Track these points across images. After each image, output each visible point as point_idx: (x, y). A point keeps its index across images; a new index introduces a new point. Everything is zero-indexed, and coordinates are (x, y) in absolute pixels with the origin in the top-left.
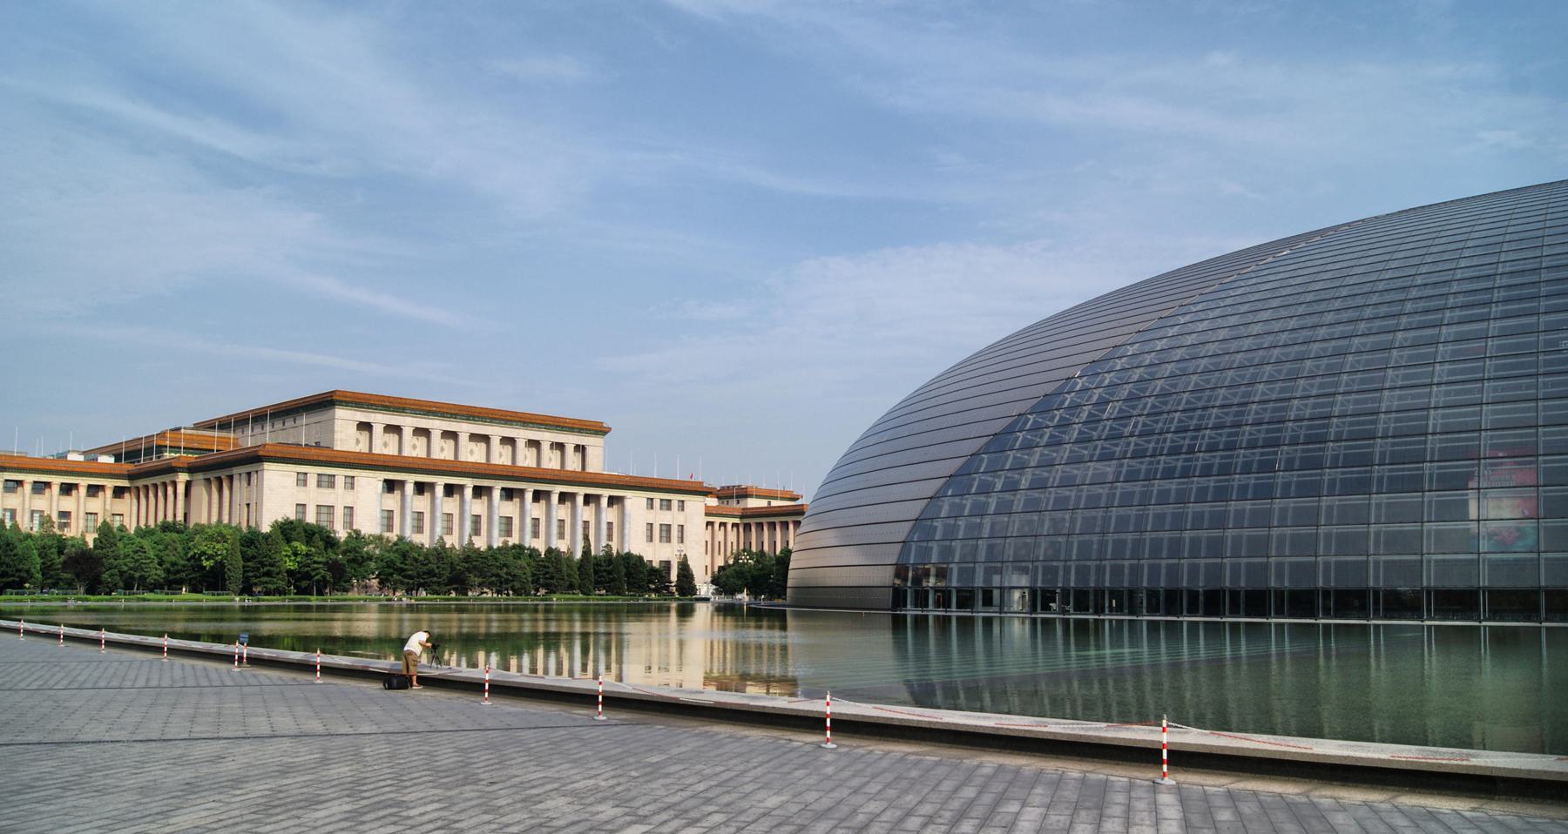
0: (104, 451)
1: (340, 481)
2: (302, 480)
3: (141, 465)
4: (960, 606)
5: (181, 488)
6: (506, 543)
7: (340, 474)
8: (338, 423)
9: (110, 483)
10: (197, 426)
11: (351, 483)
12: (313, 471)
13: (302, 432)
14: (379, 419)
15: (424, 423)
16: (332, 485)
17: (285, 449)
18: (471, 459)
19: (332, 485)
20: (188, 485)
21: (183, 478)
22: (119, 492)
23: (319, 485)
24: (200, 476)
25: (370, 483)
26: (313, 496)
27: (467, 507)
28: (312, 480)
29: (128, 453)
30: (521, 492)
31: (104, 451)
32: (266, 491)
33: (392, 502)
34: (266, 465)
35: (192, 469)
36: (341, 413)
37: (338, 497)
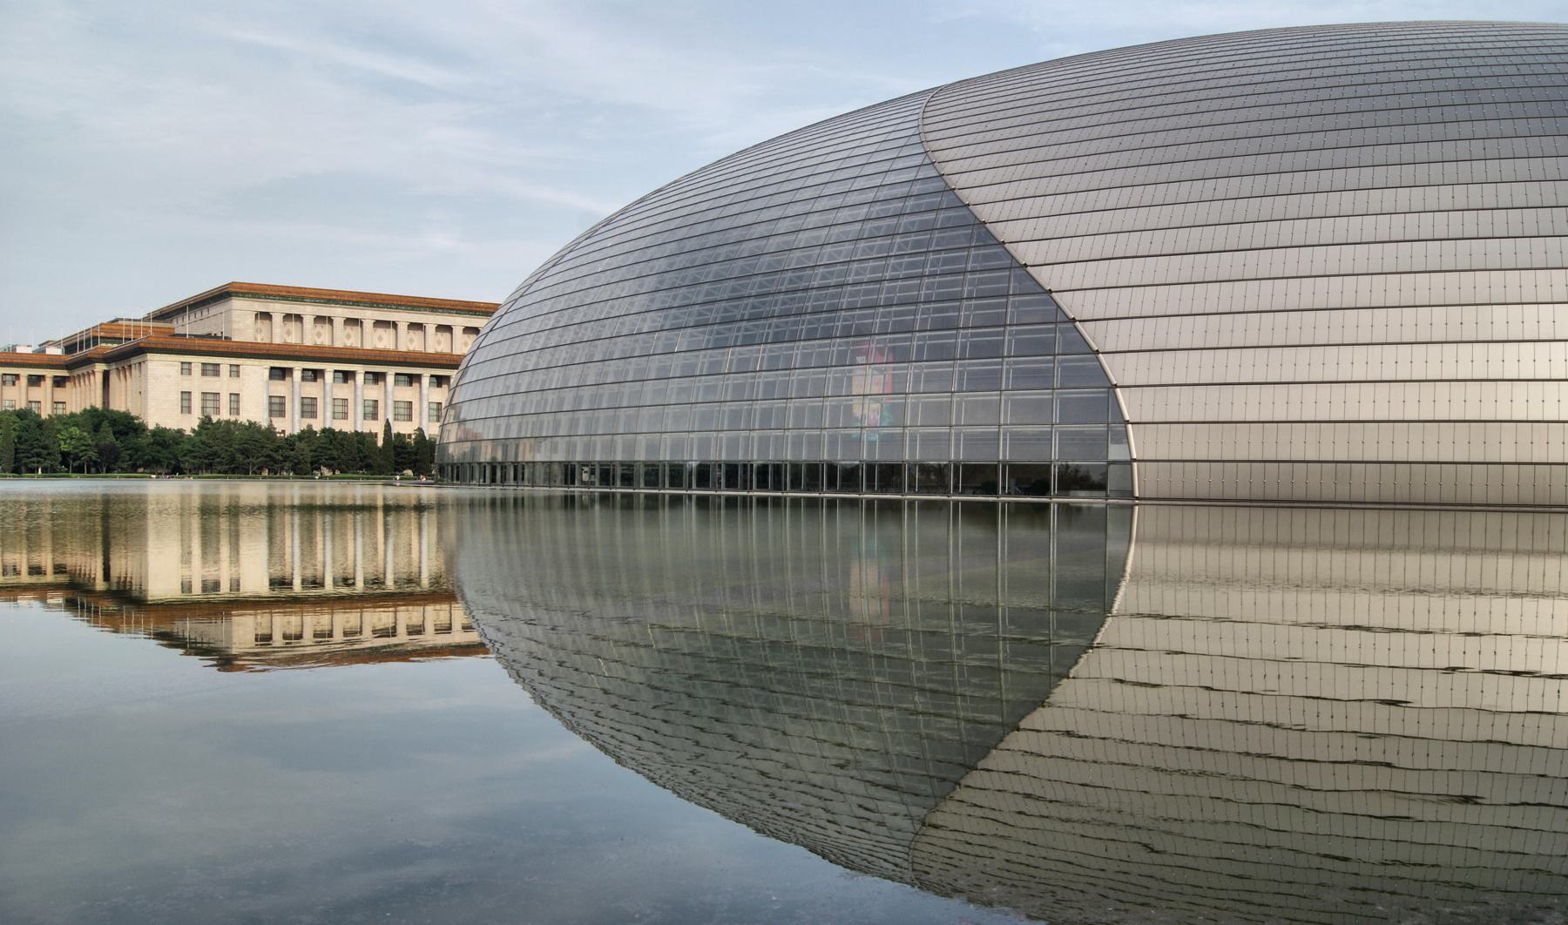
0: (56, 344)
1: (225, 370)
2: (186, 369)
3: (77, 357)
4: (648, 484)
5: (99, 377)
6: (310, 426)
7: (225, 363)
8: (235, 315)
9: (50, 374)
10: (146, 319)
11: (235, 371)
12: (197, 361)
13: (187, 326)
14: (278, 309)
15: (325, 311)
16: (216, 373)
17: (197, 341)
18: (380, 346)
19: (216, 373)
20: (106, 375)
21: (100, 368)
22: (59, 382)
23: (204, 373)
24: (114, 366)
25: (255, 372)
26: (198, 384)
27: (359, 393)
28: (197, 370)
29: (70, 348)
30: (418, 377)
31: (56, 344)
32: (151, 380)
33: (280, 388)
34: (150, 356)
35: (107, 359)
36: (237, 303)
37: (223, 384)
